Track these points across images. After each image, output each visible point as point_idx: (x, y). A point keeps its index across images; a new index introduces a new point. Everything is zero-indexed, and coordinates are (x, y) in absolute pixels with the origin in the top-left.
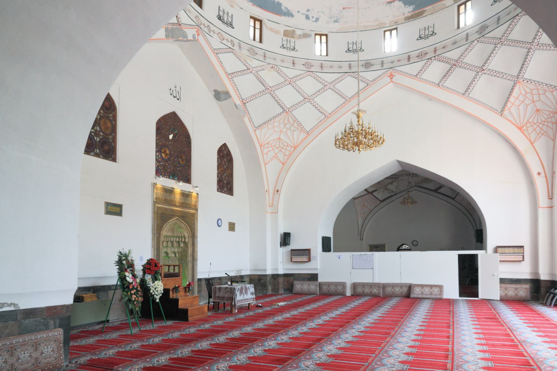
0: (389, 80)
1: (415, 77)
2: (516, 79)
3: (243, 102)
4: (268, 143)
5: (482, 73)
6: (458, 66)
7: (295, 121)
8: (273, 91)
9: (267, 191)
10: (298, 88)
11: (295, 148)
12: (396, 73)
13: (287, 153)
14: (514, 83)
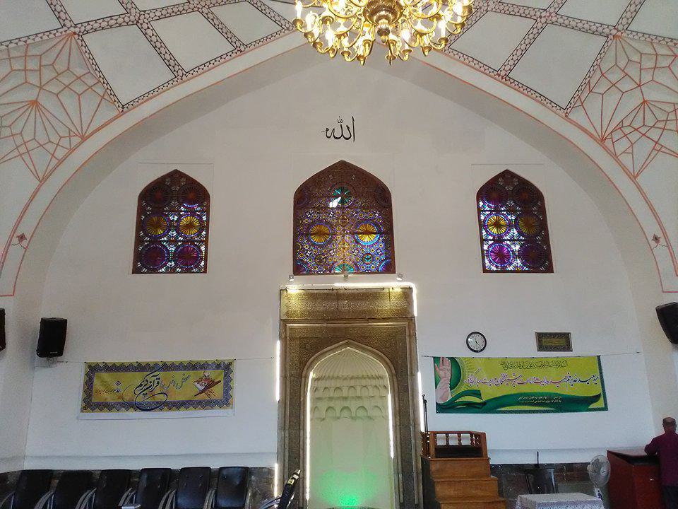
3: (499, 75)
4: (620, 126)
7: (652, 43)
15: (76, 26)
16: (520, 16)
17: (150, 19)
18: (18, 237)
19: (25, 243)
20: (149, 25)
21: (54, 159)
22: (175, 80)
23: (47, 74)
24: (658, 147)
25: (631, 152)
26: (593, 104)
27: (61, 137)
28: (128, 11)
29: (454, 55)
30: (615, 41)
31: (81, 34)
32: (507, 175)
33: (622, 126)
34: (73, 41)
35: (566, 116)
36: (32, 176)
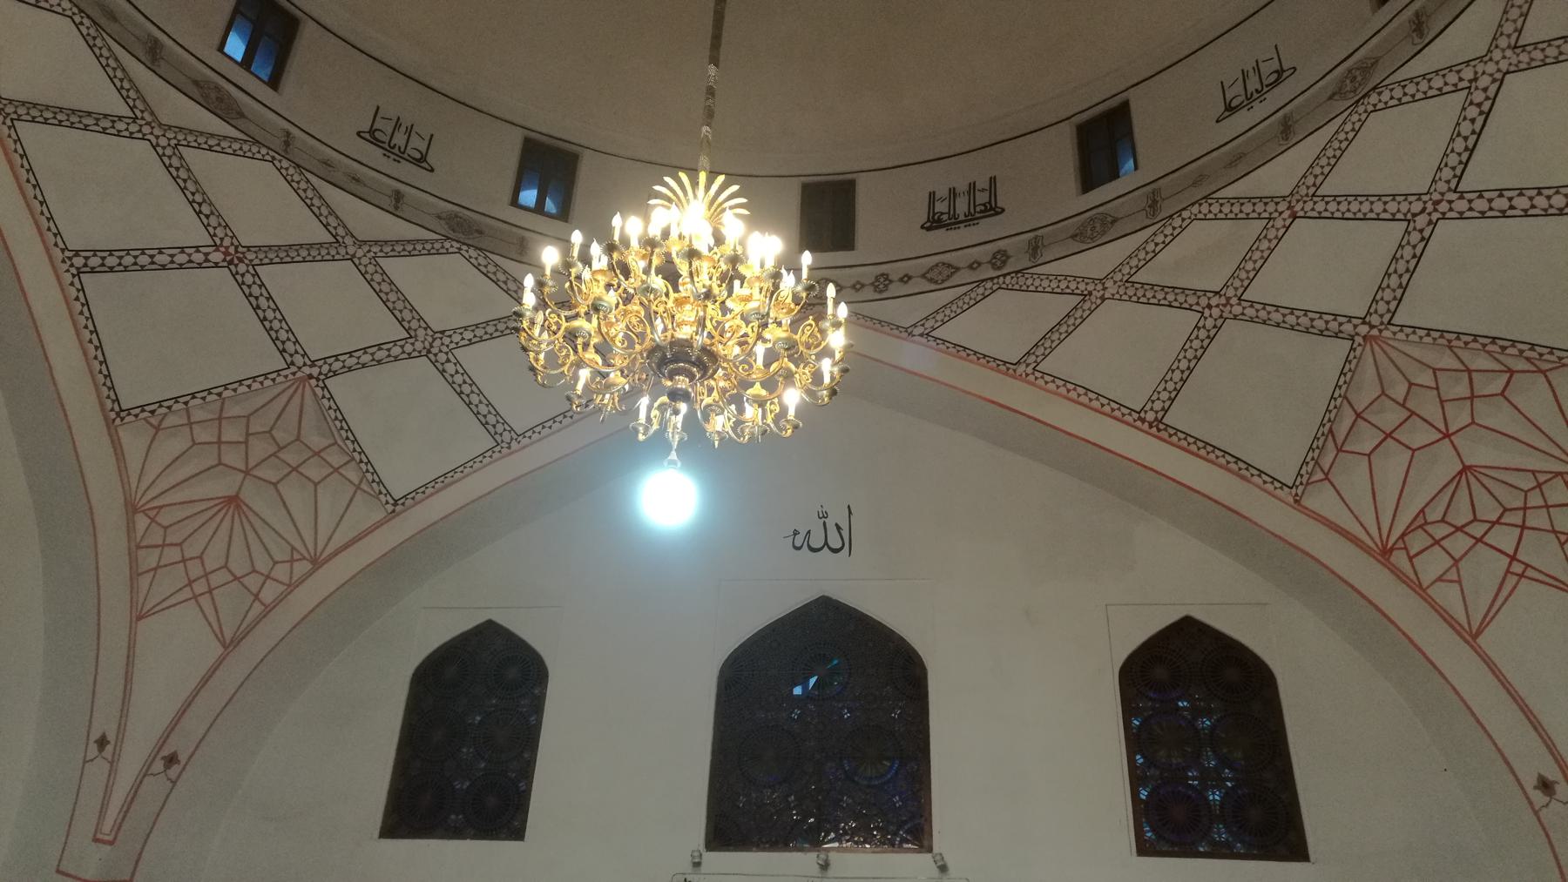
3: (1143, 420)
4: (1421, 522)
7: (1450, 348)
8: (1234, 301)
15: (313, 365)
16: (1170, 306)
17: (453, 346)
18: (163, 758)
19: (174, 771)
20: (450, 355)
21: (257, 604)
22: (496, 449)
23: (259, 449)
24: (1517, 568)
25: (1455, 577)
26: (1353, 477)
27: (276, 563)
28: (413, 334)
29: (1046, 383)
30: (1368, 347)
31: (322, 377)
32: (1187, 632)
33: (1426, 523)
34: (308, 390)
35: (1296, 501)
36: (212, 637)
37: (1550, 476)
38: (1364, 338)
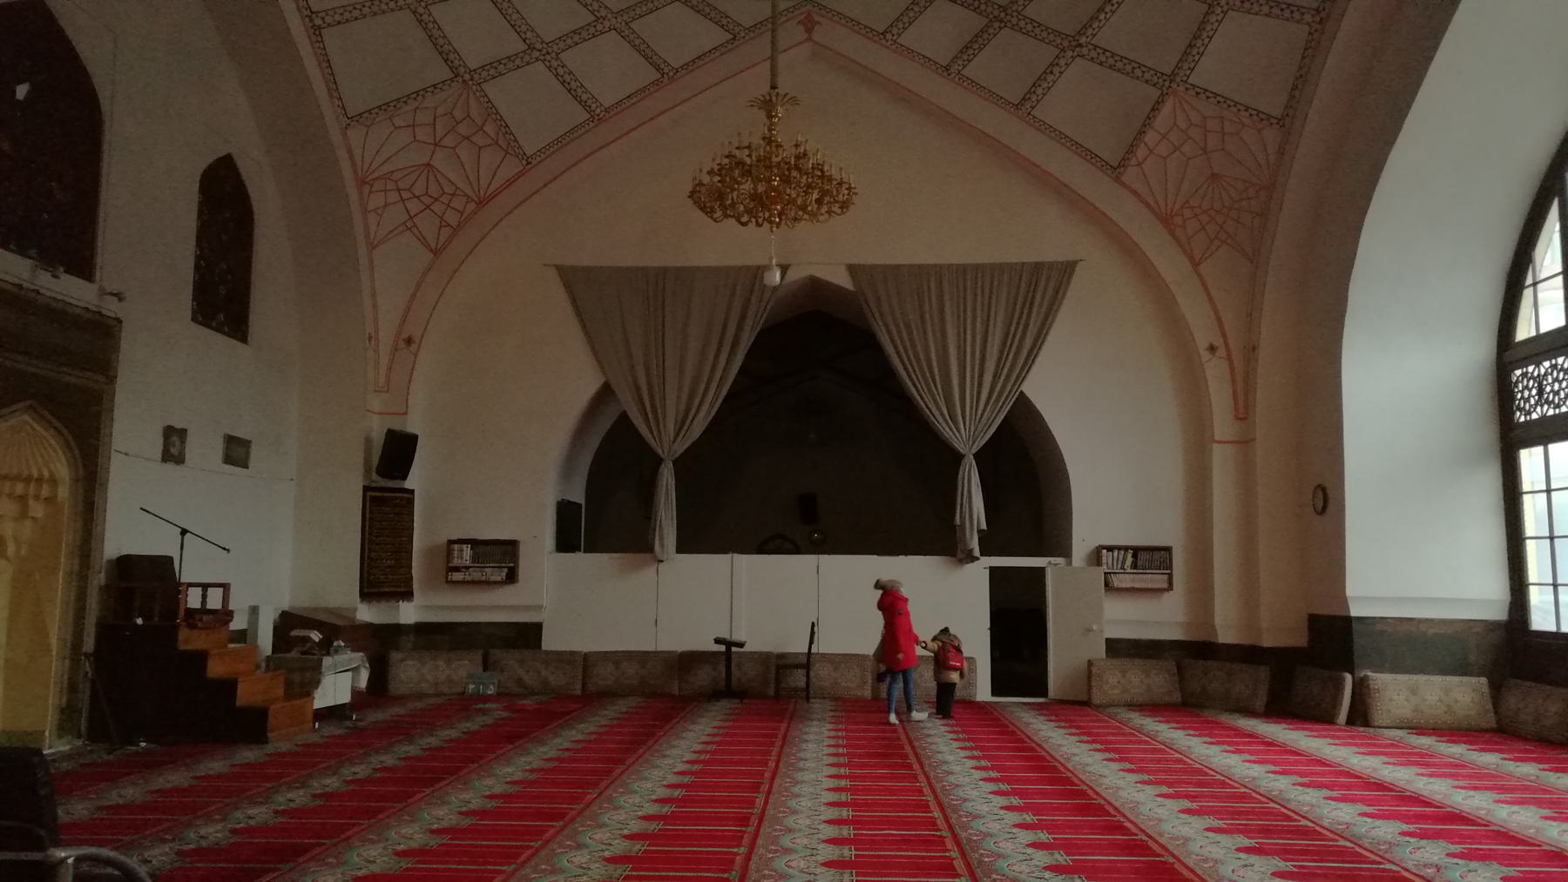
0: (800, 34)
1: (882, 37)
2: (1167, 84)
3: (311, 20)
5: (1075, 54)
6: (1009, 25)
9: (370, 338)
10: (510, 11)
11: (482, 203)
12: (823, 17)
13: (452, 218)
14: (1160, 92)
24: (409, 224)
37: (462, 194)
38: (464, 81)
